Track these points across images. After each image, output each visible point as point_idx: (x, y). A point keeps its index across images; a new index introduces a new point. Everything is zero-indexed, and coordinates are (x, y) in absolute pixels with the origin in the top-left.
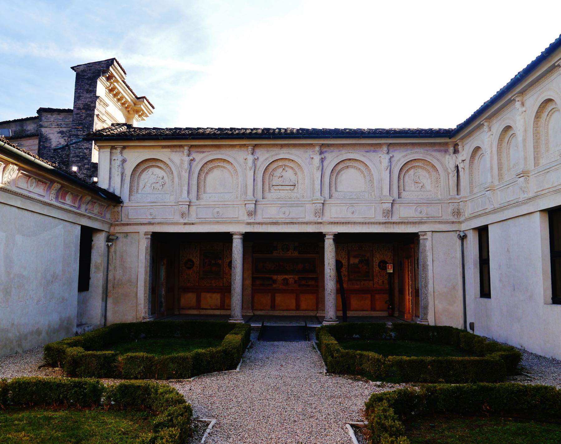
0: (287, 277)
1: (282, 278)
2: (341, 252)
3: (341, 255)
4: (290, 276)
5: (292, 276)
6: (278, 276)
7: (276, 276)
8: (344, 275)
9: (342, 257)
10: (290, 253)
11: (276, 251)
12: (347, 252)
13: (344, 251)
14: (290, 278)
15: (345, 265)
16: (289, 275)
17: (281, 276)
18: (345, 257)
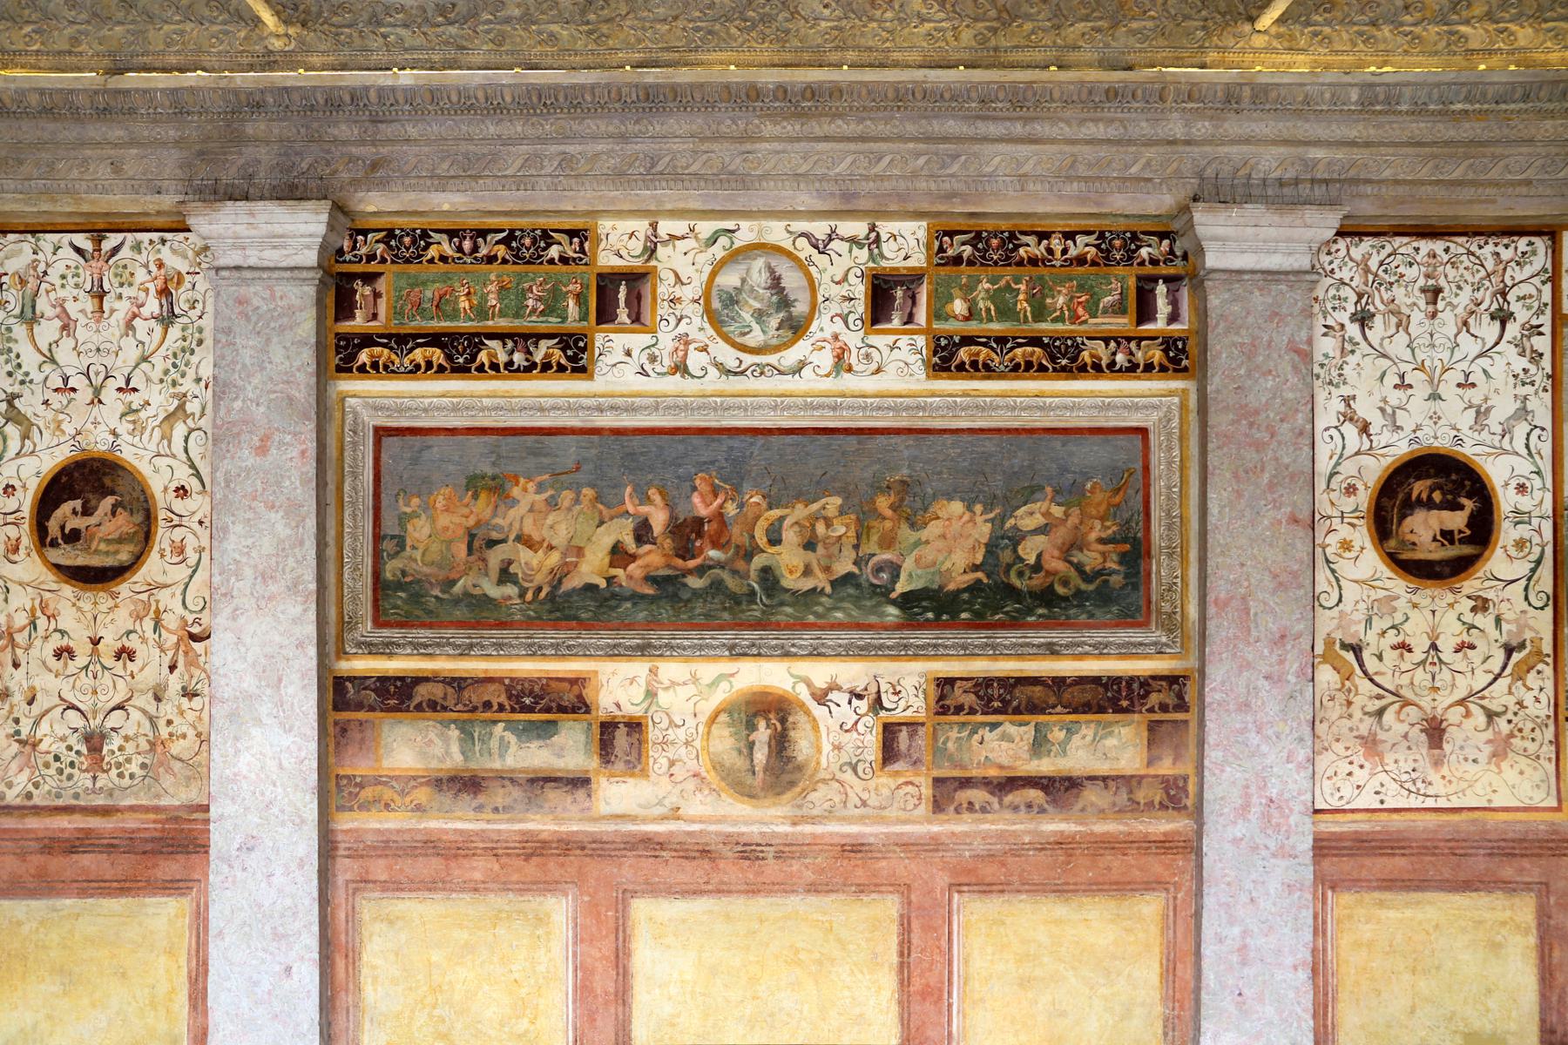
0: (773, 675)
1: (720, 696)
2: (1469, 346)
3: (1467, 384)
4: (821, 672)
5: (853, 672)
6: (671, 669)
7: (638, 668)
8: (1509, 650)
9: (1481, 414)
10: (826, 359)
11: (638, 341)
12: (1543, 344)
13: (1513, 329)
14: (821, 698)
15: (1521, 517)
16: (816, 654)
17: (708, 670)
18: (1523, 412)
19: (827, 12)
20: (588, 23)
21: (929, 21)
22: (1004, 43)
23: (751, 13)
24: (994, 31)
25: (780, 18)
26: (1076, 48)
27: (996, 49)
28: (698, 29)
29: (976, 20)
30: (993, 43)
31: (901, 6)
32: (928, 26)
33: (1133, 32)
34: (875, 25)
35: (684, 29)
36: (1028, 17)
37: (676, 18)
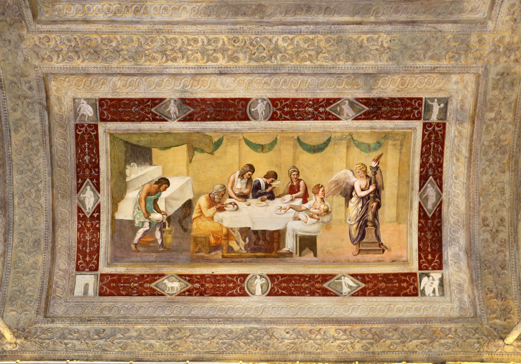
19: (288, 335)
20: (170, 339)
21: (339, 339)
22: (377, 350)
23: (251, 336)
24: (372, 344)
25: (265, 338)
26: (414, 352)
27: (373, 353)
28: (224, 343)
29: (362, 339)
30: (371, 350)
31: (325, 333)
32: (338, 342)
33: (443, 345)
34: (312, 341)
35: (217, 343)
36: (388, 338)
37: (213, 338)
